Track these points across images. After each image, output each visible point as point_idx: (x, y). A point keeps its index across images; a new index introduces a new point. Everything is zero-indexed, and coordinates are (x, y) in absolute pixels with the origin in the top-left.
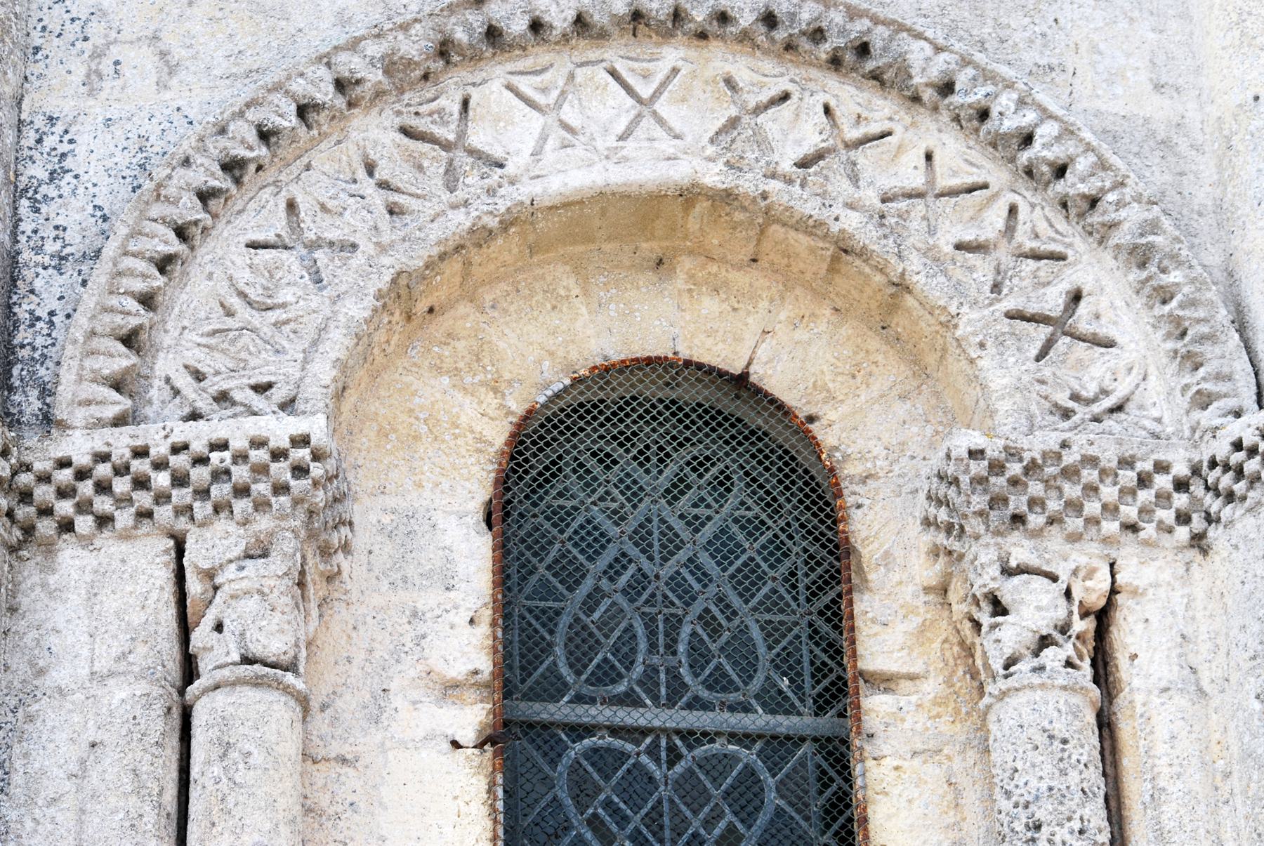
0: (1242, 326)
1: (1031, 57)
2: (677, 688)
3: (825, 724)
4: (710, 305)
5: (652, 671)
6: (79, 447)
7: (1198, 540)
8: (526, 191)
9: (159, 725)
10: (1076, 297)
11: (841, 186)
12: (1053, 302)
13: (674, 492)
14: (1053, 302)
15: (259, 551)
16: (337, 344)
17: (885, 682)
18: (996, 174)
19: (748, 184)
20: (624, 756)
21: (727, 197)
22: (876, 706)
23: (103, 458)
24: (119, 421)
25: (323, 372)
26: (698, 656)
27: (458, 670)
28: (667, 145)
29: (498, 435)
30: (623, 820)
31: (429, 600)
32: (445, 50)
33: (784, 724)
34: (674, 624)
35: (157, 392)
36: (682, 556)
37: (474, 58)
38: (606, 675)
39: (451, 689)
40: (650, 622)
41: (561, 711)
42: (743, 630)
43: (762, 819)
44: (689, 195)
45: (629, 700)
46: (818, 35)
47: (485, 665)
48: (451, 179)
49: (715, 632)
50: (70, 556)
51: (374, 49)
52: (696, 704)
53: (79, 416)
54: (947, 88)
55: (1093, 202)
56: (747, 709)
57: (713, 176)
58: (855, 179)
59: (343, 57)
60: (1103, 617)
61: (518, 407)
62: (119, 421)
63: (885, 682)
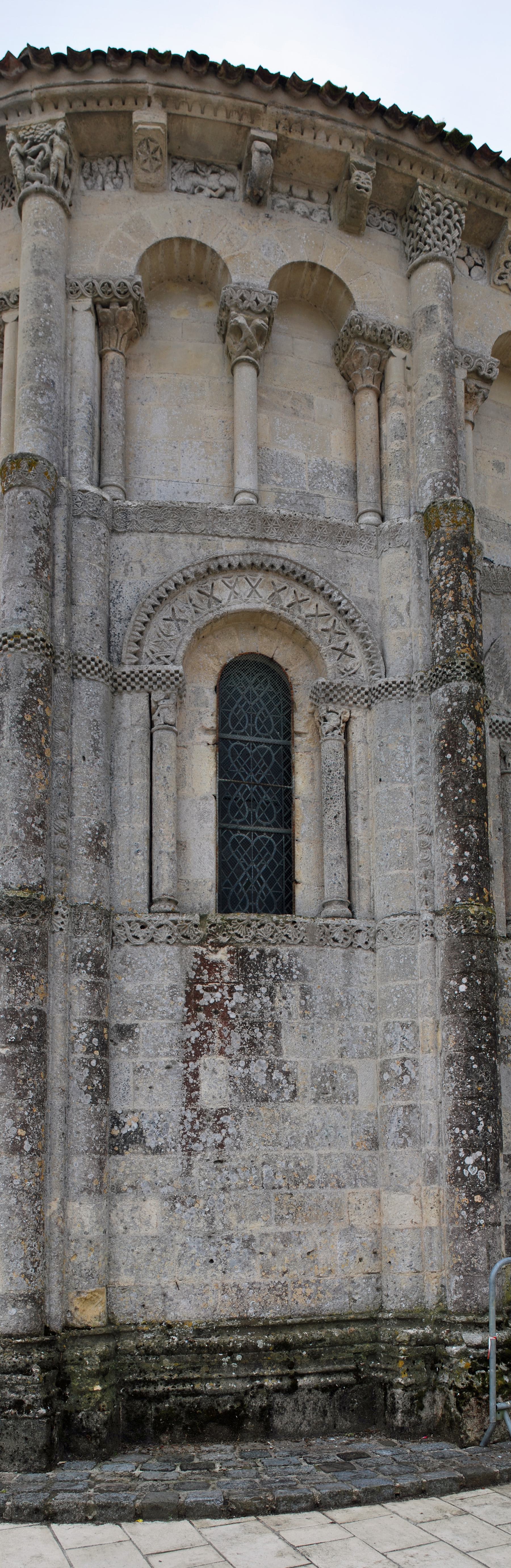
0: (383, 654)
1: (342, 581)
2: (254, 731)
3: (285, 742)
4: (265, 639)
5: (249, 727)
6: (127, 669)
7: (369, 707)
8: (226, 609)
10: (347, 644)
11: (297, 613)
12: (342, 645)
13: (255, 684)
14: (342, 645)
16: (184, 646)
17: (299, 734)
18: (332, 612)
19: (276, 610)
20: (242, 747)
21: (271, 614)
22: (298, 739)
23: (133, 672)
24: (136, 664)
25: (181, 653)
26: (259, 724)
27: (209, 726)
28: (258, 599)
29: (218, 669)
30: (242, 763)
31: (203, 709)
32: (208, 570)
33: (277, 741)
34: (254, 716)
35: (144, 656)
36: (256, 700)
37: (215, 573)
38: (239, 728)
39: (207, 731)
40: (249, 715)
41: (229, 736)
42: (269, 719)
43: (271, 764)
44: (263, 612)
45: (244, 734)
46: (294, 572)
47: (214, 725)
48: (209, 606)
49: (263, 719)
50: (126, 697)
51: (192, 569)
52: (258, 736)
53: (127, 661)
54: (322, 589)
55: (353, 621)
56: (268, 737)
57: (268, 608)
58: (300, 611)
59: (185, 571)
60: (347, 723)
61: (223, 662)
62: (136, 664)
63: (299, 734)
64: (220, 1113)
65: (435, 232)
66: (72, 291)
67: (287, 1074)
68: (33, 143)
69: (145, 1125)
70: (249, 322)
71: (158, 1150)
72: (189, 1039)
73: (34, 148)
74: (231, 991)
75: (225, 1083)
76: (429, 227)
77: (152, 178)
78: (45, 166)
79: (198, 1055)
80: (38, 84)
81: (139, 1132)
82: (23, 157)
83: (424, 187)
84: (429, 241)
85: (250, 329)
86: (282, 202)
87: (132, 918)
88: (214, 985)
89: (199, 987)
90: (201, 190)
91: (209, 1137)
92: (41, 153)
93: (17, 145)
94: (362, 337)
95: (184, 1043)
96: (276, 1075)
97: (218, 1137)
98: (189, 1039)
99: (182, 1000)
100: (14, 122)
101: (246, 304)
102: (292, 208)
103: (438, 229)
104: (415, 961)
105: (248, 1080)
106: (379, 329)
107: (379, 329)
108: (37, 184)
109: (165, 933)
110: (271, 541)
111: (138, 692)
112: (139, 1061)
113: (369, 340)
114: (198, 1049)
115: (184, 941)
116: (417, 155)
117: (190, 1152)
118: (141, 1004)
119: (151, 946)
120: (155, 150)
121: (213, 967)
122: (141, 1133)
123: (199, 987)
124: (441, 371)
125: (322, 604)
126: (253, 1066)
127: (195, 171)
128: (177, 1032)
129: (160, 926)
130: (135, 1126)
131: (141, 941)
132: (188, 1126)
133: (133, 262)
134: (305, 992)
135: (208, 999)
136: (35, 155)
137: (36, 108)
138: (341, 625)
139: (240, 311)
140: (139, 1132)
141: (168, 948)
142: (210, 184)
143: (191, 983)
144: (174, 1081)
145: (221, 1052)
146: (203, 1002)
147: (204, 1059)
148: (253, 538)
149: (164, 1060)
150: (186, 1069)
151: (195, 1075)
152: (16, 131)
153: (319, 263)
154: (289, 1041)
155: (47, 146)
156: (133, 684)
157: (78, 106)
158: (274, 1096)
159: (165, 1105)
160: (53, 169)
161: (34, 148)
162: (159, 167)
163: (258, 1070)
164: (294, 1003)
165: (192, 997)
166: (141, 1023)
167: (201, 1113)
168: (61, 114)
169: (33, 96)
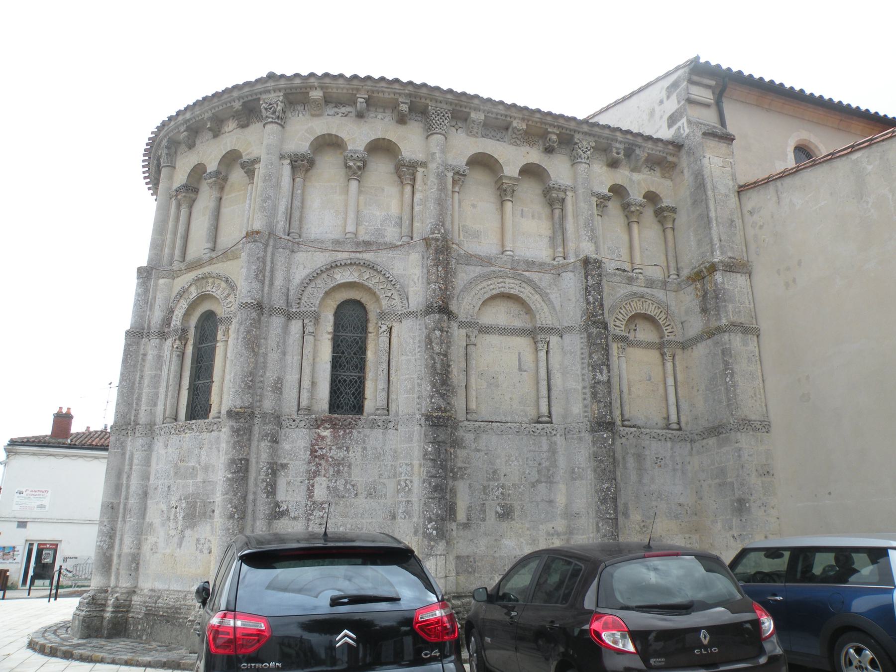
0: (407, 299)
1: (391, 267)
4: (357, 292)
6: (294, 310)
7: (401, 321)
8: (339, 282)
9: (301, 339)
11: (370, 282)
12: (389, 295)
14: (389, 295)
15: (310, 321)
16: (319, 299)
18: (386, 281)
19: (361, 281)
21: (359, 283)
24: (298, 308)
25: (318, 302)
27: (329, 331)
28: (353, 277)
29: (335, 306)
31: (328, 324)
32: (332, 267)
35: (302, 304)
37: (334, 267)
39: (329, 333)
44: (355, 282)
46: (369, 265)
47: (332, 331)
48: (331, 281)
50: (294, 322)
51: (325, 267)
54: (381, 271)
55: (395, 284)
57: (357, 280)
58: (371, 281)
60: (391, 328)
62: (298, 308)
65: (436, 122)
66: (282, 157)
67: (353, 486)
68: (270, 104)
70: (354, 164)
71: (295, 518)
72: (311, 470)
73: (270, 106)
74: (330, 449)
75: (325, 489)
76: (434, 121)
77: (318, 112)
78: (274, 112)
79: (314, 477)
80: (273, 84)
81: (287, 510)
82: (266, 109)
83: (432, 106)
84: (434, 126)
85: (355, 167)
86: (372, 115)
87: (290, 417)
88: (323, 446)
89: (316, 447)
90: (338, 114)
91: (317, 513)
93: (264, 105)
94: (404, 165)
95: (308, 471)
97: (321, 514)
98: (311, 470)
99: (309, 453)
100: (264, 96)
101: (353, 158)
102: (376, 117)
103: (438, 122)
104: (413, 435)
105: (336, 489)
106: (412, 162)
107: (412, 162)
108: (270, 120)
109: (303, 424)
112: (289, 479)
113: (407, 166)
114: (316, 474)
115: (311, 427)
116: (428, 96)
117: (309, 520)
118: (291, 454)
119: (297, 429)
121: (323, 438)
122: (288, 511)
123: (316, 447)
124: (436, 179)
125: (382, 277)
126: (338, 483)
127: (336, 107)
128: (305, 466)
129: (301, 421)
130: (286, 508)
131: (293, 427)
132: (308, 508)
133: (308, 144)
134: (365, 449)
135: (320, 452)
136: (270, 109)
137: (272, 92)
138: (389, 287)
139: (351, 160)
140: (287, 510)
141: (304, 430)
142: (342, 111)
144: (304, 487)
145: (324, 476)
146: (318, 454)
147: (317, 479)
149: (299, 479)
150: (309, 483)
151: (313, 486)
152: (264, 100)
153: (386, 138)
154: (355, 471)
155: (275, 106)
157: (288, 91)
159: (299, 499)
160: (277, 114)
161: (270, 106)
163: (340, 484)
164: (359, 454)
165: (313, 451)
166: (291, 462)
167: (314, 503)
168: (281, 94)
169: (271, 88)
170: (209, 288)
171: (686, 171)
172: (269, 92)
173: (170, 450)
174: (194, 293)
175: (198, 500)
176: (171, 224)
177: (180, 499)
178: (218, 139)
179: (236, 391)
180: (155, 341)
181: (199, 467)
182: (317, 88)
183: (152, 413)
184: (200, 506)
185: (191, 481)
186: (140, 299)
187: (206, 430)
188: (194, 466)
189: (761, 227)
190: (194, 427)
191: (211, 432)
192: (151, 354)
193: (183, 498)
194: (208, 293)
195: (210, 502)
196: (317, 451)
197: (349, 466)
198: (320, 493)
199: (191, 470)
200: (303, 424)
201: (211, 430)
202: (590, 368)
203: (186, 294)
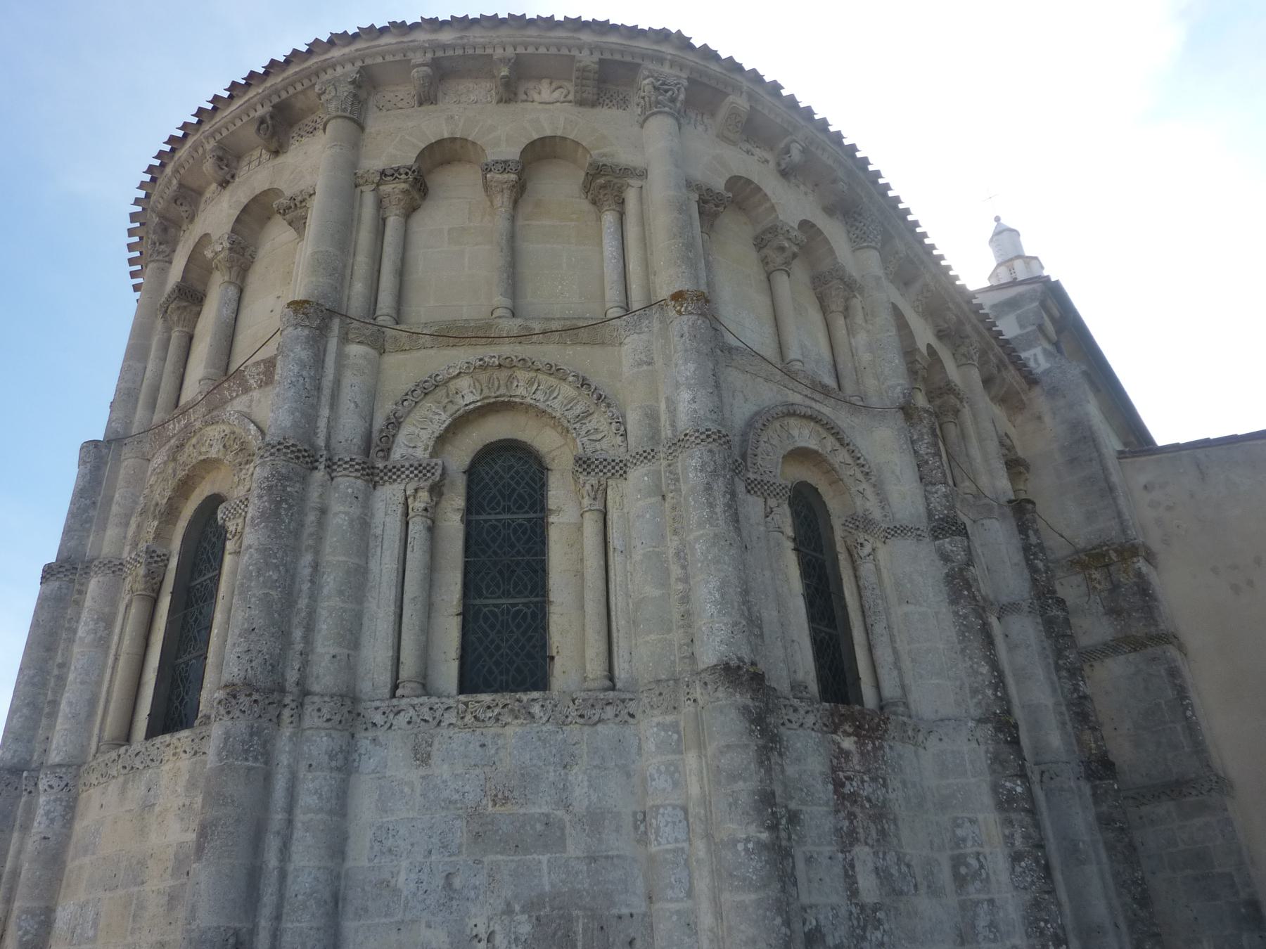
53: (751, 470)
64: (876, 908)
67: (908, 866)
69: (823, 922)
72: (842, 828)
78: (673, 100)
81: (818, 928)
82: (657, 89)
92: (670, 93)
95: (838, 830)
96: (904, 869)
98: (842, 828)
99: (831, 787)
108: (667, 109)
110: (816, 401)
111: (758, 496)
115: (825, 729)
120: (739, 122)
128: (831, 818)
130: (814, 923)
132: (855, 923)
135: (848, 789)
137: (667, 64)
141: (813, 734)
143: (834, 770)
145: (867, 844)
148: (806, 396)
149: (827, 850)
150: (844, 859)
151: (853, 867)
156: (756, 489)
158: (905, 889)
159: (834, 899)
162: (737, 132)
166: (804, 808)
167: (862, 908)
170: (521, 391)
171: (1047, 419)
172: (661, 60)
173: (441, 770)
174: (468, 394)
175: (575, 913)
176: (364, 236)
177: (509, 911)
178: (512, 107)
179: (736, 624)
180: (348, 483)
181: (567, 818)
182: (744, 93)
183: (349, 664)
184: (585, 930)
185: (544, 859)
186: (304, 373)
187: (579, 720)
188: (547, 816)
189: (1169, 508)
190: (536, 709)
191: (595, 724)
192: (341, 514)
193: (517, 908)
194: (517, 400)
195: (620, 917)
196: (843, 785)
197: (895, 821)
198: (868, 885)
199: (539, 827)
200: (810, 720)
201: (596, 718)
202: (1064, 673)
203: (441, 392)
